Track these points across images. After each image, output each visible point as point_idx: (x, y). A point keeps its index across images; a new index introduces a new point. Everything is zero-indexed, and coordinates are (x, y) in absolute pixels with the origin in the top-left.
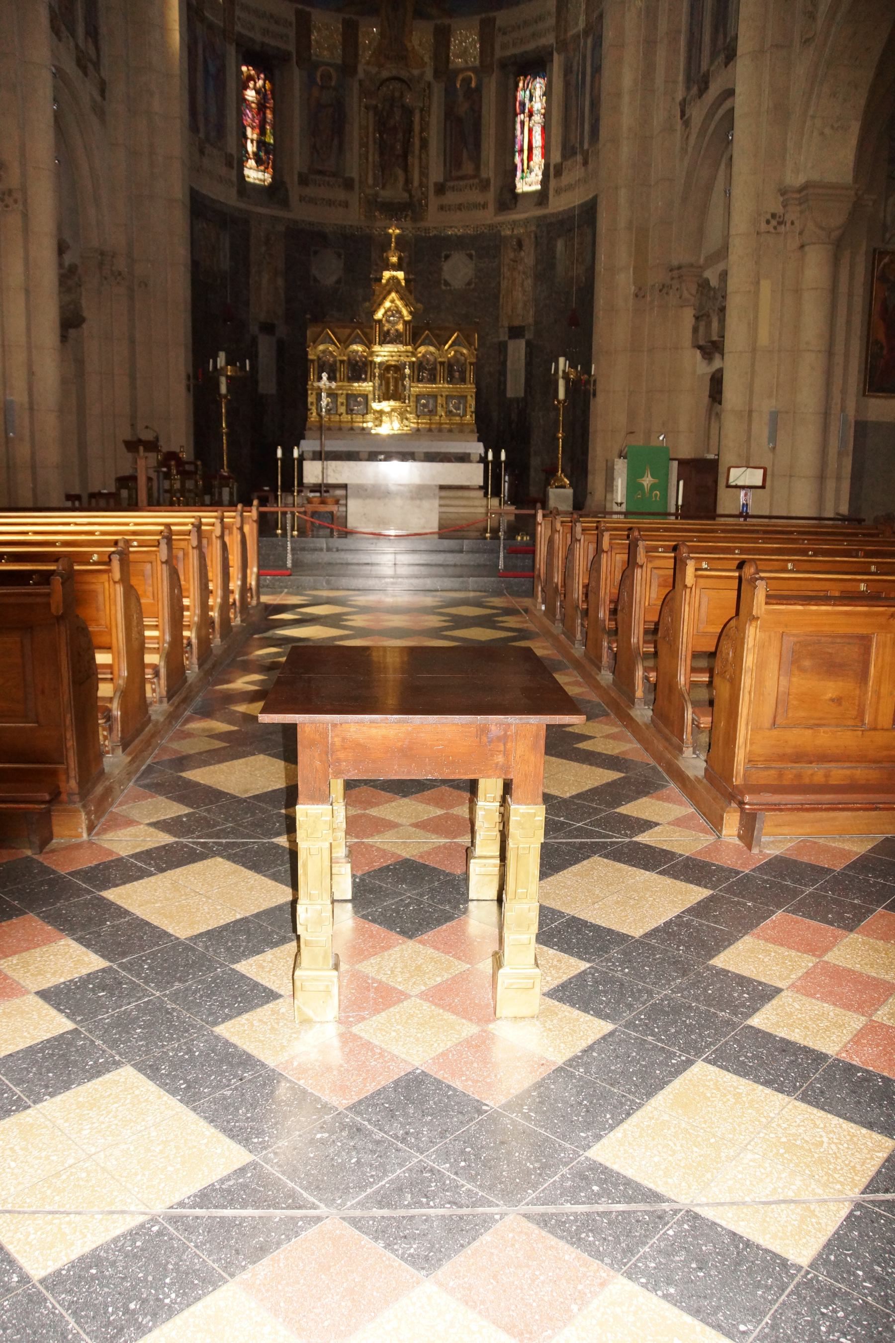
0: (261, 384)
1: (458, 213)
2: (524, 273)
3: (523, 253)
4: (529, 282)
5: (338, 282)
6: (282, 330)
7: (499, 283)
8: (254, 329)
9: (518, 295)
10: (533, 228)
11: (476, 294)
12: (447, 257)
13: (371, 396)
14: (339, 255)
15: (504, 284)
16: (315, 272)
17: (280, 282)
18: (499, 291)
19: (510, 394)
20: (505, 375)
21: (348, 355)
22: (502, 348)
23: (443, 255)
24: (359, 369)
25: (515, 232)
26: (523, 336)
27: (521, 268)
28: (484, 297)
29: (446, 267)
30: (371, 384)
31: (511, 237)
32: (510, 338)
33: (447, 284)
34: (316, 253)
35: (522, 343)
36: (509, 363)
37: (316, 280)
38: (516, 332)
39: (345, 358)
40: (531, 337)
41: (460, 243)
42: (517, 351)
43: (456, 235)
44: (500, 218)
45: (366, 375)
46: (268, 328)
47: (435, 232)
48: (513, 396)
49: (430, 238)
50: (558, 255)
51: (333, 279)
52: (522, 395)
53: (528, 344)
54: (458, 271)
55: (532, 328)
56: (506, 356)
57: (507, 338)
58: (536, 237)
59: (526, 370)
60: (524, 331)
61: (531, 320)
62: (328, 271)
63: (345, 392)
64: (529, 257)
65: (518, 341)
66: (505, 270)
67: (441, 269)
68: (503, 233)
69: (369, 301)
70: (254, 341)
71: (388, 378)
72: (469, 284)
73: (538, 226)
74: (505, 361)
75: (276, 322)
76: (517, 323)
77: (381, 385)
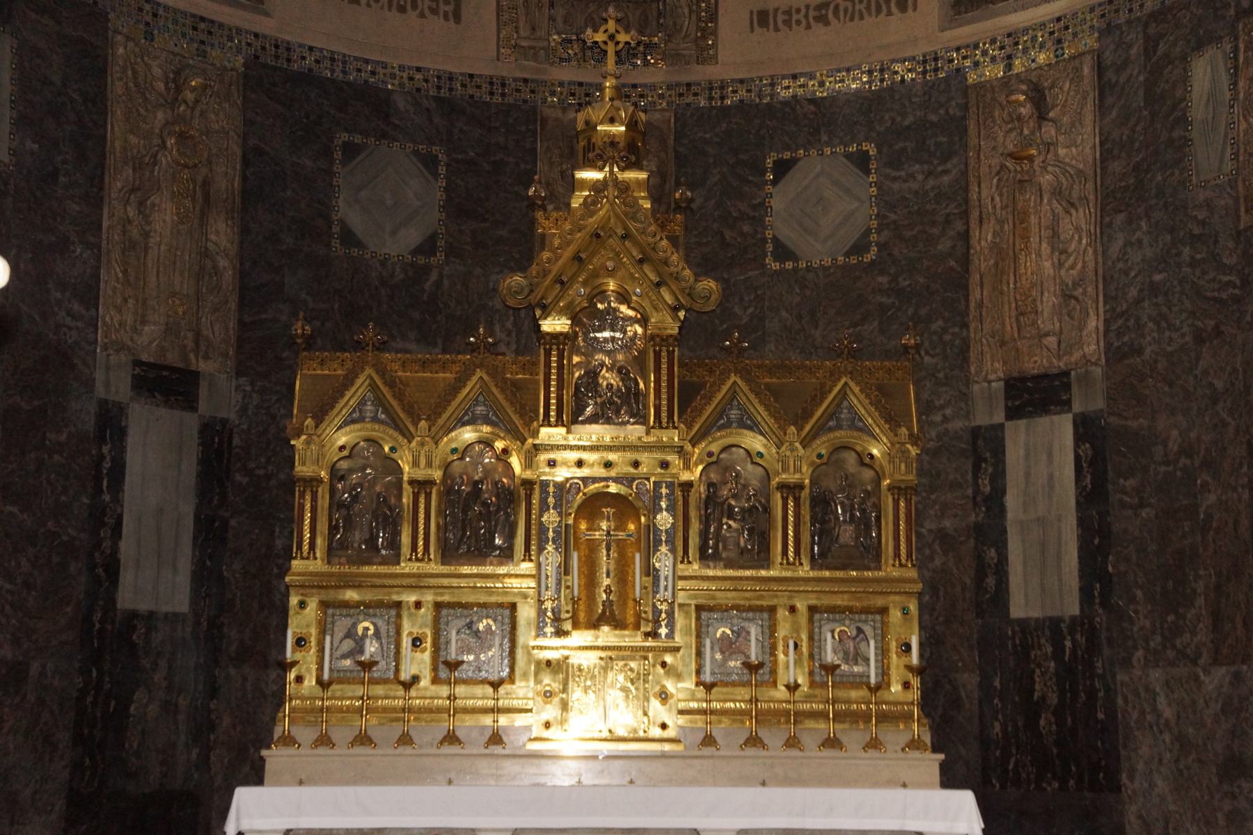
0: (127, 578)
1: (819, 29)
2: (1057, 192)
3: (1049, 131)
4: (1078, 225)
5: (427, 247)
6: (222, 394)
7: (965, 236)
8: (114, 382)
9: (1039, 263)
10: (1090, 42)
11: (883, 280)
12: (782, 169)
13: (526, 613)
14: (430, 163)
15: (983, 238)
16: (347, 211)
17: (222, 234)
18: (965, 261)
19: (1021, 606)
20: (1001, 544)
21: (447, 467)
22: (985, 449)
23: (769, 162)
24: (482, 518)
25: (1018, 65)
26: (1066, 405)
27: (1046, 179)
28: (906, 305)
29: (780, 199)
30: (527, 567)
31: (1006, 84)
32: (1012, 414)
33: (783, 252)
34: (351, 151)
35: (1062, 428)
36: (1012, 501)
37: (348, 237)
38: (1034, 395)
39: (437, 475)
40: (1099, 403)
41: (817, 120)
42: (1042, 461)
43: (813, 101)
44: (964, 33)
45: (510, 537)
46: (168, 384)
47: (742, 93)
48: (1035, 613)
49: (725, 110)
50: (1198, 111)
51: (412, 236)
52: (1072, 607)
53: (1086, 429)
54: (822, 210)
55: (1098, 371)
56: (999, 475)
57: (999, 417)
58: (1100, 69)
59: (1082, 522)
60: (1067, 387)
61: (1092, 348)
62: (390, 209)
63: (429, 598)
64: (1075, 144)
65: (1043, 422)
66: (986, 193)
67: (763, 206)
68: (972, 78)
69: (522, 267)
70: (111, 423)
71: (593, 546)
72: (859, 248)
73: (1107, 31)
74: (999, 492)
75: (203, 366)
76: (1037, 362)
77: (565, 569)
